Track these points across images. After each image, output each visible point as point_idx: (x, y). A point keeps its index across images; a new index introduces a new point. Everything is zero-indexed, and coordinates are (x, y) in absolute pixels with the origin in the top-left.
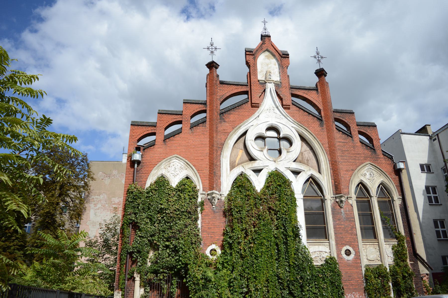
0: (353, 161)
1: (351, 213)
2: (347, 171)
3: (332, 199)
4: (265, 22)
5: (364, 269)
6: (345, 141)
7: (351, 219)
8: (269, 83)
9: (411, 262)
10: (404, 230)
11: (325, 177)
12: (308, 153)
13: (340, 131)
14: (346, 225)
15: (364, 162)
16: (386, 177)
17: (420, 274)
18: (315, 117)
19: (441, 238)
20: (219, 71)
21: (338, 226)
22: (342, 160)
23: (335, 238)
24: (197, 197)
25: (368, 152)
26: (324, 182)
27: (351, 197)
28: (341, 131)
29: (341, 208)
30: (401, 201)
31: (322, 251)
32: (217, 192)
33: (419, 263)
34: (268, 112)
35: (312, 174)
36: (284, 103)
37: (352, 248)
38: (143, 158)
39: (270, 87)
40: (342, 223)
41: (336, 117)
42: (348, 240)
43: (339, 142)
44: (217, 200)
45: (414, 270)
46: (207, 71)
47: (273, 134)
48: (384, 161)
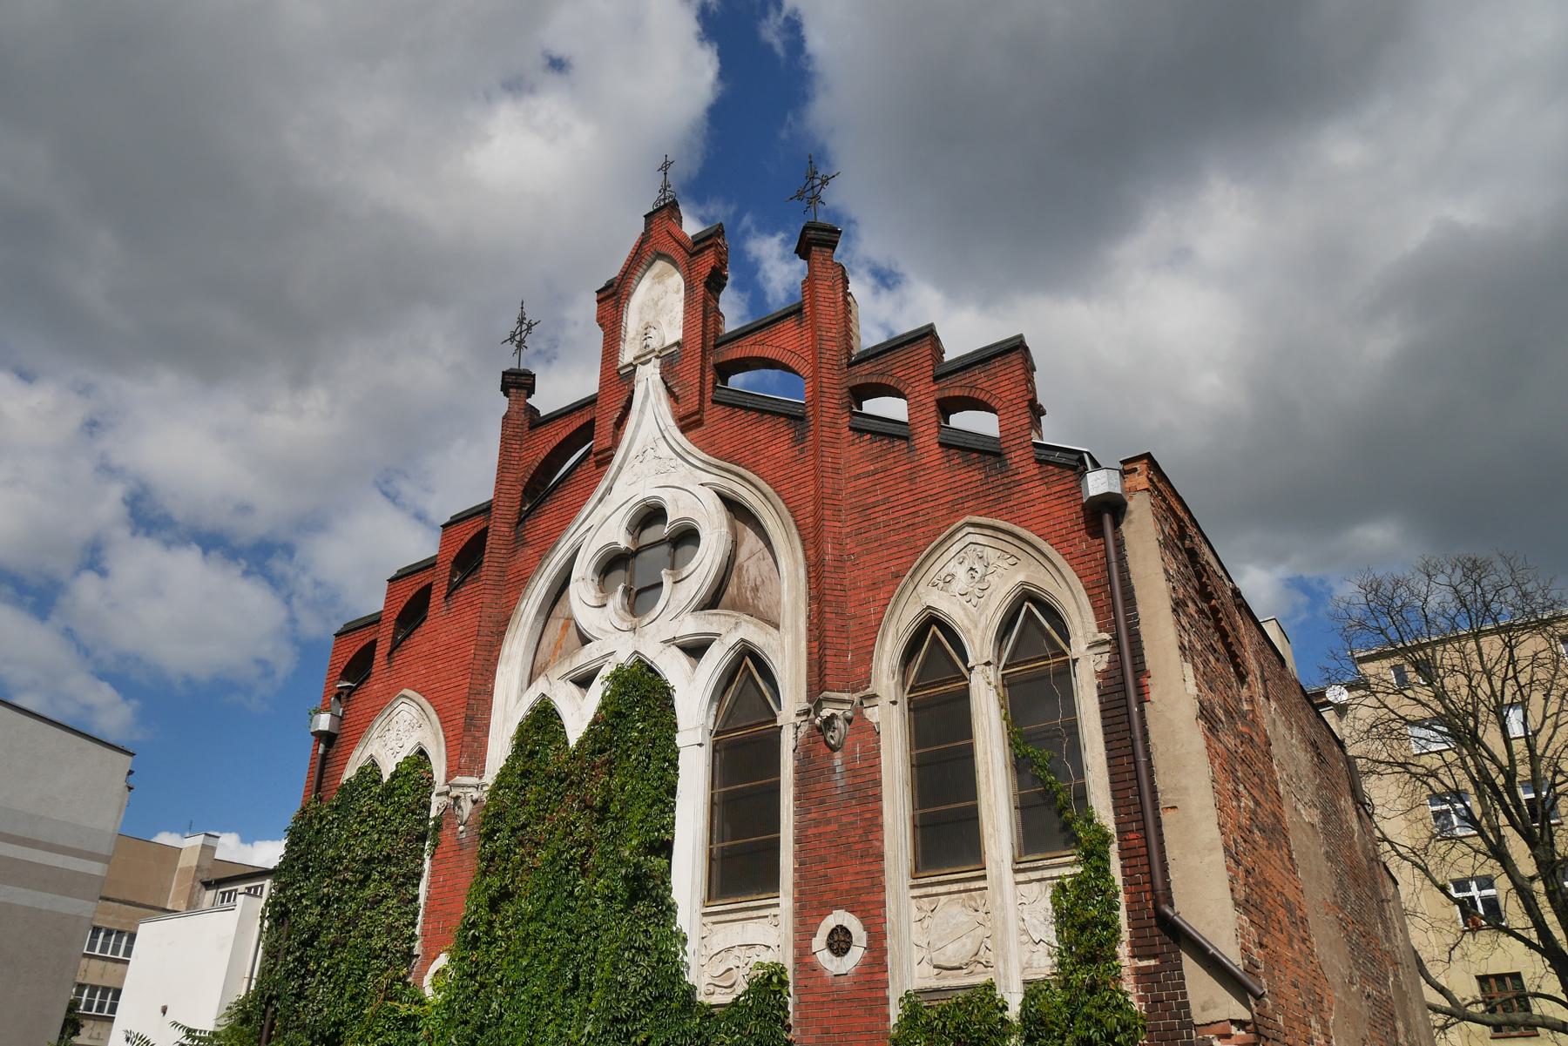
0: (905, 535)
1: (870, 762)
2: (874, 586)
3: (798, 721)
5: (895, 1013)
6: (877, 465)
7: (867, 792)
8: (643, 364)
9: (1145, 963)
10: (1114, 797)
11: (788, 639)
12: (759, 559)
14: (844, 820)
15: (948, 526)
16: (1042, 559)
17: (1191, 1025)
18: (781, 415)
21: (815, 831)
22: (858, 549)
23: (796, 885)
24: (427, 807)
26: (780, 656)
27: (875, 696)
28: (869, 432)
29: (834, 749)
30: (1106, 657)
31: (753, 946)
32: (474, 780)
33: (1189, 964)
34: (637, 464)
35: (742, 640)
37: (862, 919)
38: (344, 722)
39: (649, 378)
40: (830, 814)
41: (858, 381)
42: (846, 886)
43: (858, 477)
45: (1157, 1001)
46: (502, 404)
48: (1038, 490)
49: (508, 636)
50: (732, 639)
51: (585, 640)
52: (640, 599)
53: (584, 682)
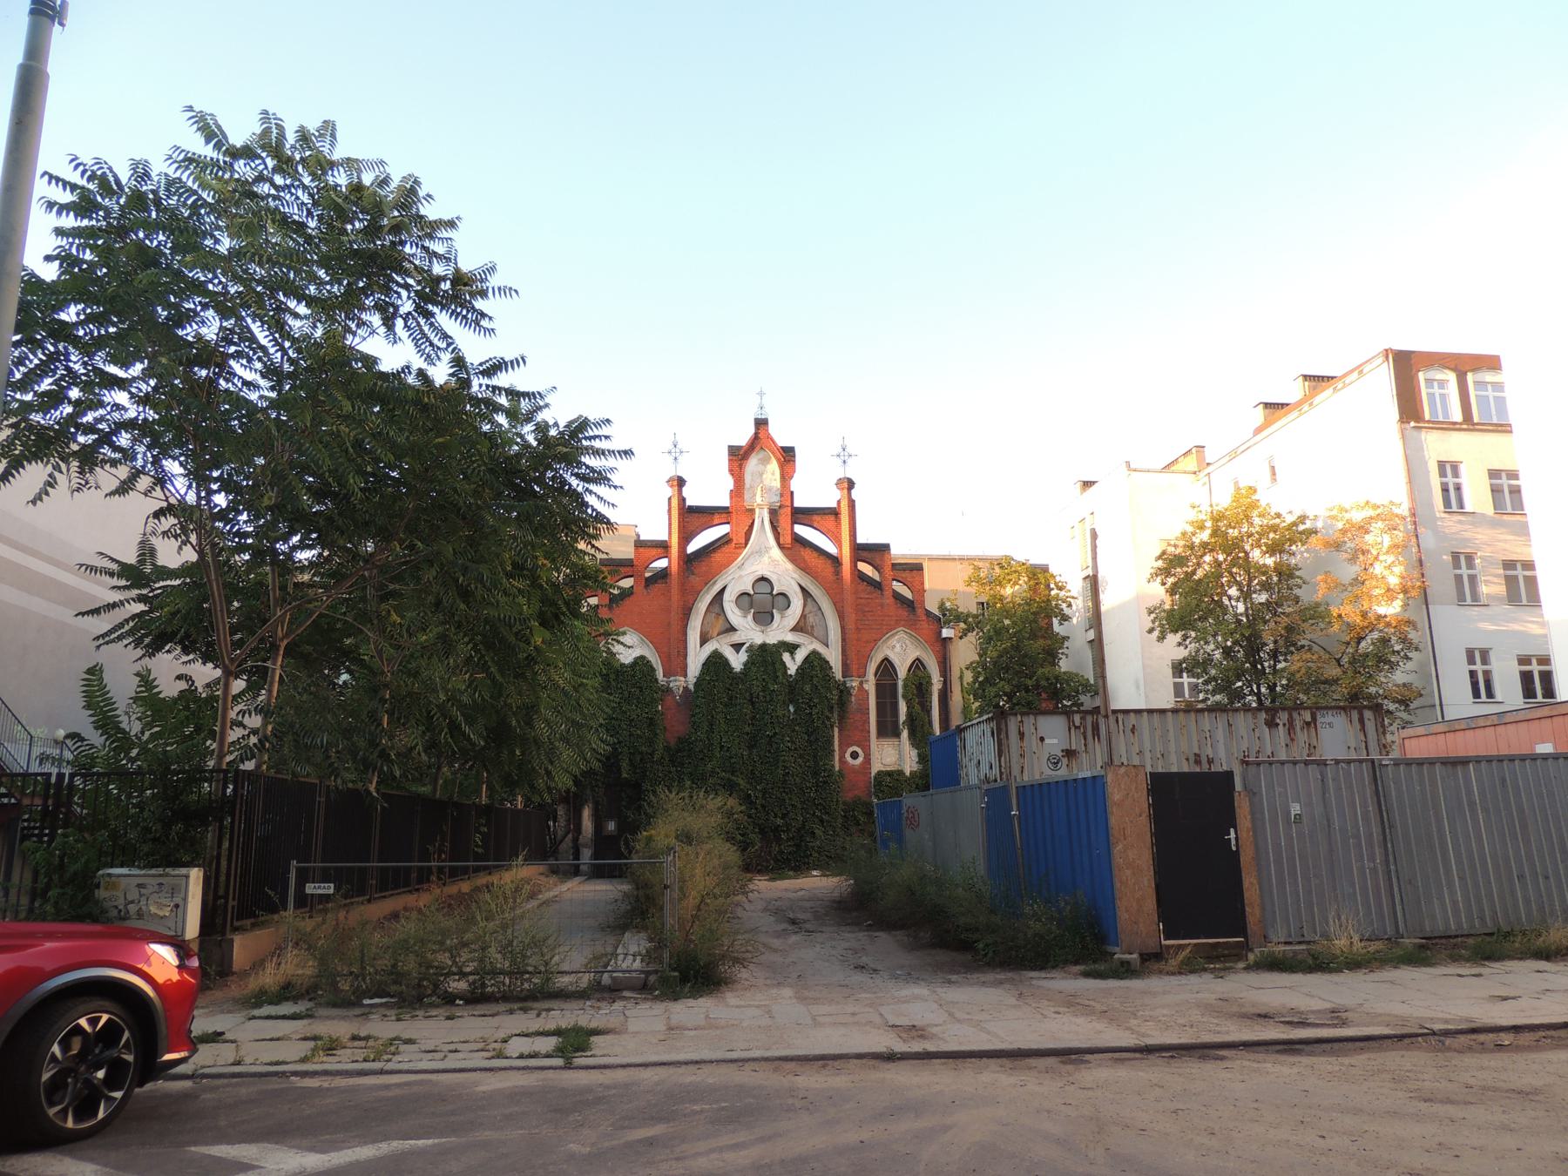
4: (761, 394)
13: (863, 581)
19: (1535, 697)
20: (686, 491)
25: (904, 613)
32: (682, 679)
36: (781, 542)
44: (681, 689)
46: (668, 491)
47: (764, 588)
49: (692, 617)
50: (811, 648)
51: (732, 629)
52: (764, 617)
53: (737, 647)
